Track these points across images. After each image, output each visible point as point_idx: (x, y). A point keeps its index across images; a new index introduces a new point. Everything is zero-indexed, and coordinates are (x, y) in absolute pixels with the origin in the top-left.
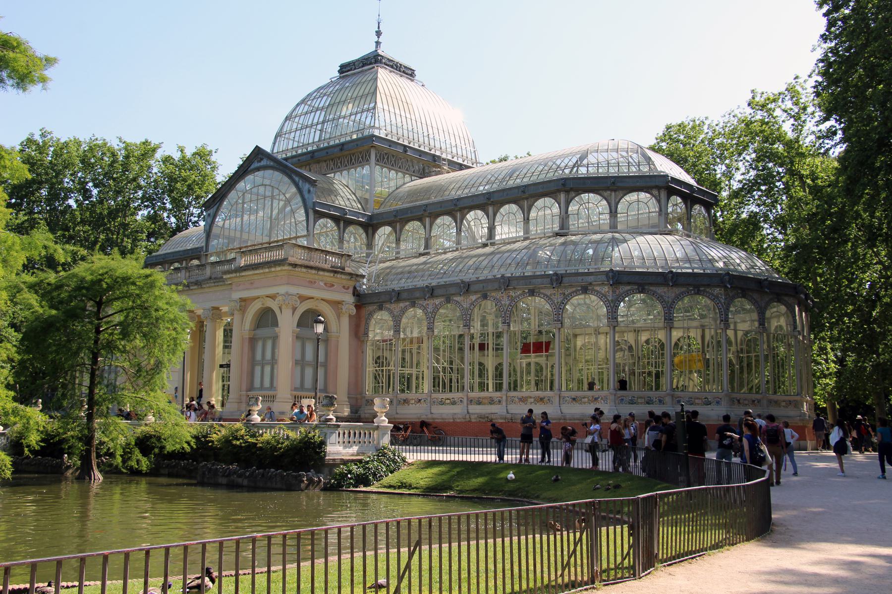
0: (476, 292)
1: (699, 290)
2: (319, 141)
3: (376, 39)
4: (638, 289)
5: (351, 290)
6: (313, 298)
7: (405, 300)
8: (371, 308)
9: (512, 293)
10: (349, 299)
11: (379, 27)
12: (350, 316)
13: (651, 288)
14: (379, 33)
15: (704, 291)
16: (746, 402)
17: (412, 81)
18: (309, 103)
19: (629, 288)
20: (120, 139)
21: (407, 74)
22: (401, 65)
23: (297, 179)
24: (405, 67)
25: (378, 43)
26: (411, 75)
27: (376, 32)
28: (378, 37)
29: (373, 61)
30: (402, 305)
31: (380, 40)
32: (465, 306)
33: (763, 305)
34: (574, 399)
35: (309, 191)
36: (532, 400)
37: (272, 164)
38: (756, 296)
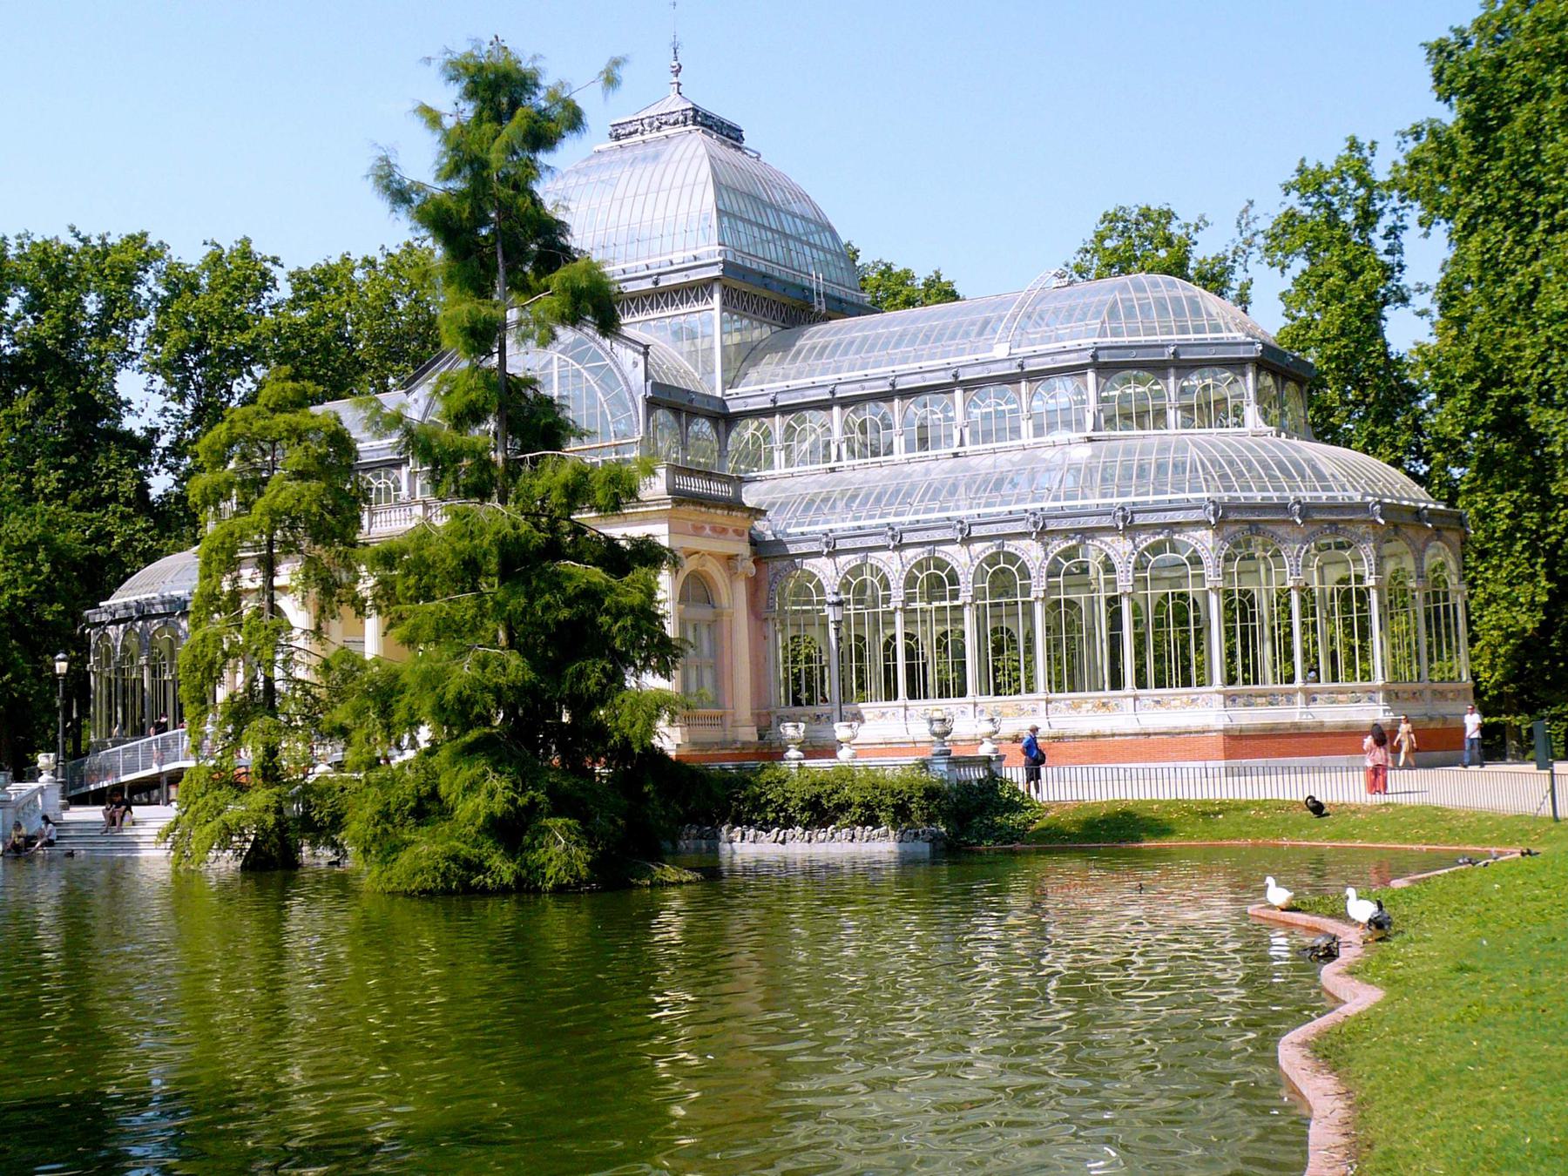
1: (1337, 529)
4: (1250, 530)
5: (746, 537)
6: (697, 553)
9: (1046, 539)
10: (744, 549)
12: (748, 579)
13: (1269, 528)
15: (1344, 529)
16: (1406, 696)
17: (739, 148)
19: (1236, 528)
20: (72, 229)
24: (729, 126)
26: (737, 140)
29: (681, 118)
32: (961, 560)
33: (1421, 547)
34: (1158, 702)
36: (1089, 706)
38: (1411, 532)
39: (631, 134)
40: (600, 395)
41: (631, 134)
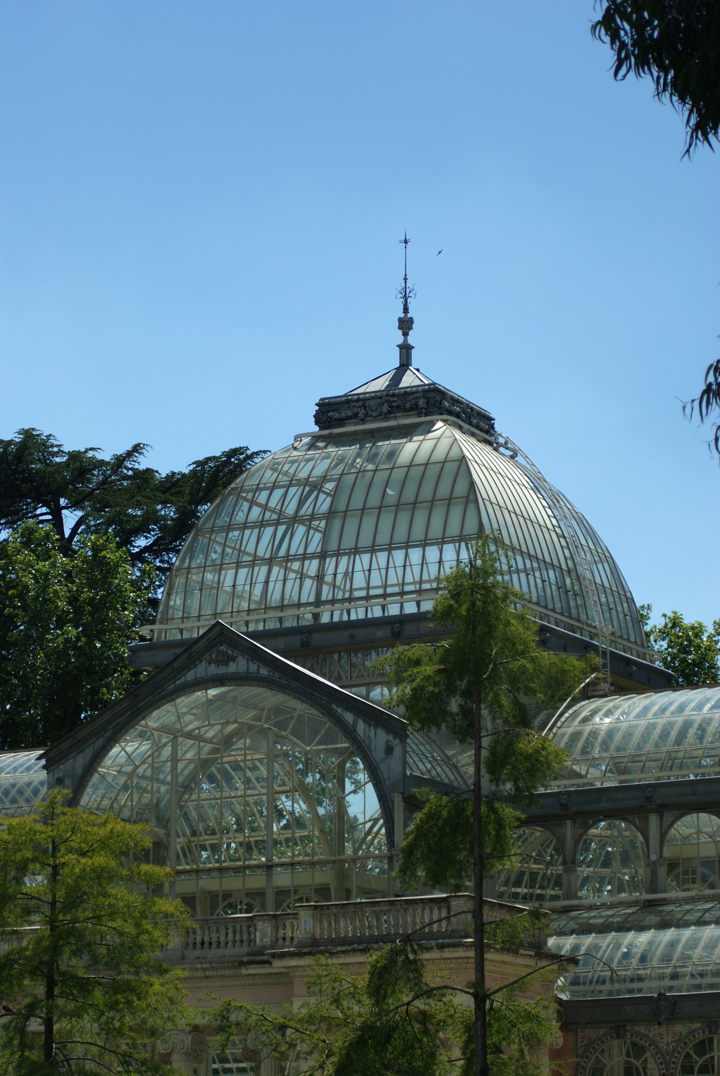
2: (318, 602)
3: (400, 340)
7: (691, 1018)
8: (591, 1033)
11: (406, 310)
14: (406, 325)
18: (262, 498)
21: (481, 430)
22: (471, 408)
23: (349, 717)
25: (406, 350)
26: (487, 432)
27: (400, 320)
28: (405, 334)
29: (422, 402)
30: (681, 1028)
31: (411, 340)
35: (389, 750)
37: (264, 671)
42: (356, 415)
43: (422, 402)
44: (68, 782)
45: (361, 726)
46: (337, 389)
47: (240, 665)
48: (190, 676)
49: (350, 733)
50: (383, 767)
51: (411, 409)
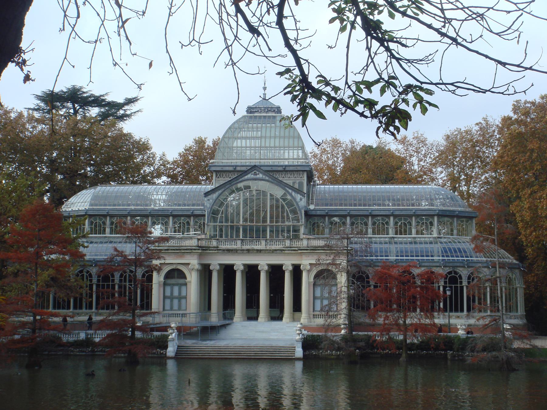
0: (424, 266)
3: (263, 92)
14: (265, 88)
23: (290, 191)
31: (266, 92)
35: (301, 199)
36: (454, 317)
37: (267, 178)
39: (256, 112)
40: (286, 207)
41: (256, 112)
42: (258, 111)
43: (276, 110)
44: (211, 201)
45: (293, 194)
46: (251, 104)
47: (260, 176)
48: (246, 177)
49: (291, 195)
50: (299, 203)
51: (273, 111)
